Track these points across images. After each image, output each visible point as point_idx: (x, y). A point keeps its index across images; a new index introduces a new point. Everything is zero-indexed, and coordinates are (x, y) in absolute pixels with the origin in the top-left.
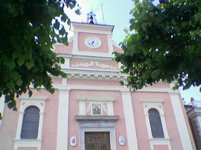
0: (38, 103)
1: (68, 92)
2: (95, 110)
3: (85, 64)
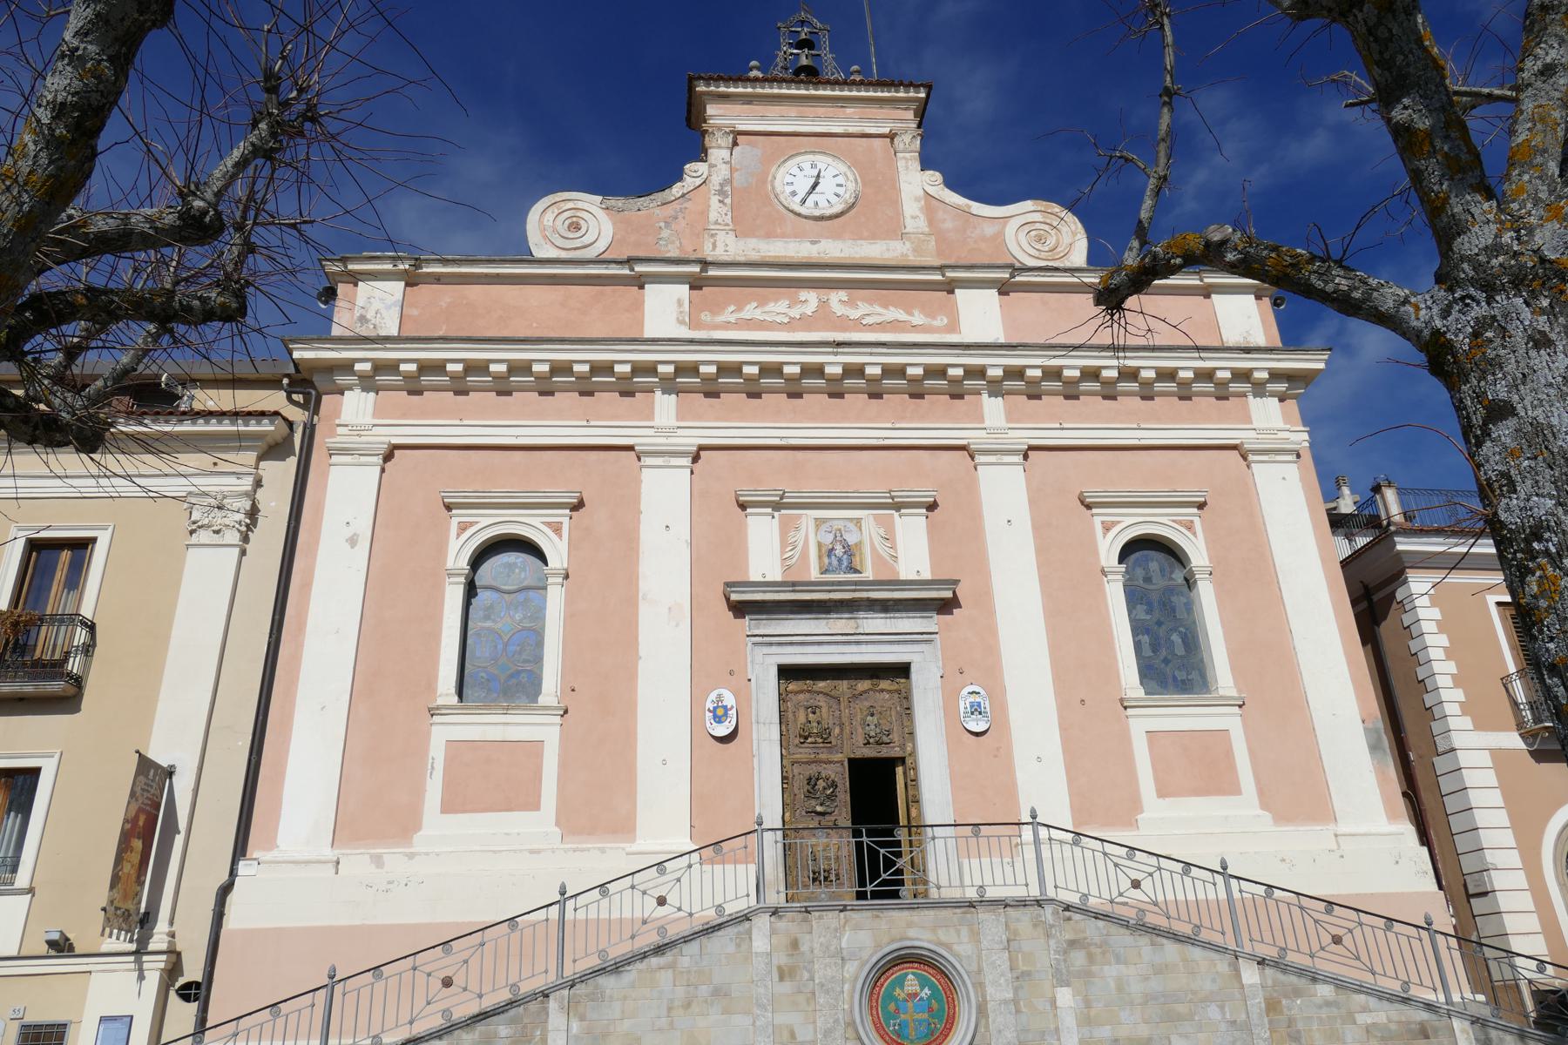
0: (536, 522)
1: (687, 461)
2: (831, 551)
3: (771, 307)
